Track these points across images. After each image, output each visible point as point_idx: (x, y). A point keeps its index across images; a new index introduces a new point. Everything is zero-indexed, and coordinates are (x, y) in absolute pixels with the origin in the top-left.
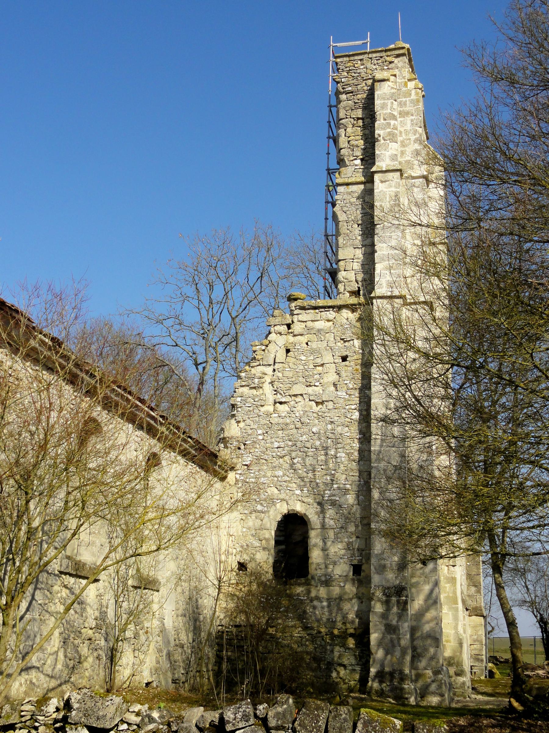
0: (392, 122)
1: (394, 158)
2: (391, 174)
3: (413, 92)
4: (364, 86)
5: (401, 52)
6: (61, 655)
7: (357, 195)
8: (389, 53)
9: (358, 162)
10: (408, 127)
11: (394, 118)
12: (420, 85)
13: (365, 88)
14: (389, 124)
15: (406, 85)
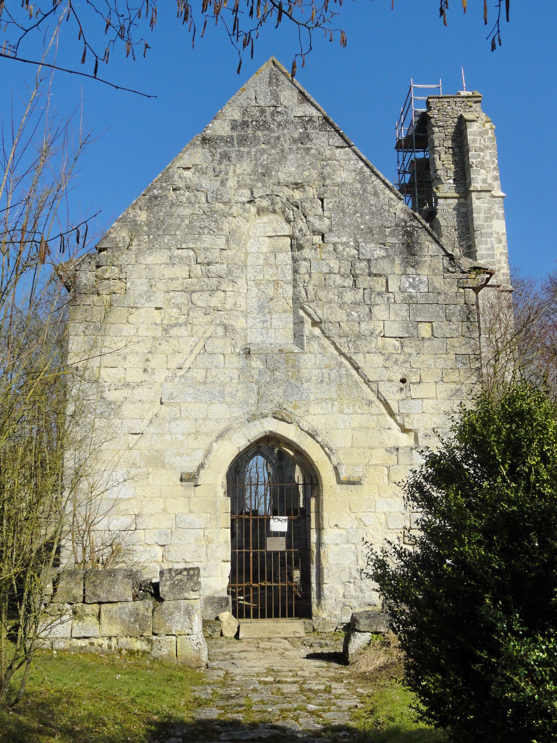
0: (482, 154)
1: (484, 181)
2: (484, 193)
3: (490, 131)
4: (452, 123)
5: (478, 99)
7: (452, 207)
8: (469, 99)
9: (451, 181)
10: (488, 158)
11: (482, 150)
12: (494, 127)
13: (453, 124)
14: (479, 155)
15: (484, 126)
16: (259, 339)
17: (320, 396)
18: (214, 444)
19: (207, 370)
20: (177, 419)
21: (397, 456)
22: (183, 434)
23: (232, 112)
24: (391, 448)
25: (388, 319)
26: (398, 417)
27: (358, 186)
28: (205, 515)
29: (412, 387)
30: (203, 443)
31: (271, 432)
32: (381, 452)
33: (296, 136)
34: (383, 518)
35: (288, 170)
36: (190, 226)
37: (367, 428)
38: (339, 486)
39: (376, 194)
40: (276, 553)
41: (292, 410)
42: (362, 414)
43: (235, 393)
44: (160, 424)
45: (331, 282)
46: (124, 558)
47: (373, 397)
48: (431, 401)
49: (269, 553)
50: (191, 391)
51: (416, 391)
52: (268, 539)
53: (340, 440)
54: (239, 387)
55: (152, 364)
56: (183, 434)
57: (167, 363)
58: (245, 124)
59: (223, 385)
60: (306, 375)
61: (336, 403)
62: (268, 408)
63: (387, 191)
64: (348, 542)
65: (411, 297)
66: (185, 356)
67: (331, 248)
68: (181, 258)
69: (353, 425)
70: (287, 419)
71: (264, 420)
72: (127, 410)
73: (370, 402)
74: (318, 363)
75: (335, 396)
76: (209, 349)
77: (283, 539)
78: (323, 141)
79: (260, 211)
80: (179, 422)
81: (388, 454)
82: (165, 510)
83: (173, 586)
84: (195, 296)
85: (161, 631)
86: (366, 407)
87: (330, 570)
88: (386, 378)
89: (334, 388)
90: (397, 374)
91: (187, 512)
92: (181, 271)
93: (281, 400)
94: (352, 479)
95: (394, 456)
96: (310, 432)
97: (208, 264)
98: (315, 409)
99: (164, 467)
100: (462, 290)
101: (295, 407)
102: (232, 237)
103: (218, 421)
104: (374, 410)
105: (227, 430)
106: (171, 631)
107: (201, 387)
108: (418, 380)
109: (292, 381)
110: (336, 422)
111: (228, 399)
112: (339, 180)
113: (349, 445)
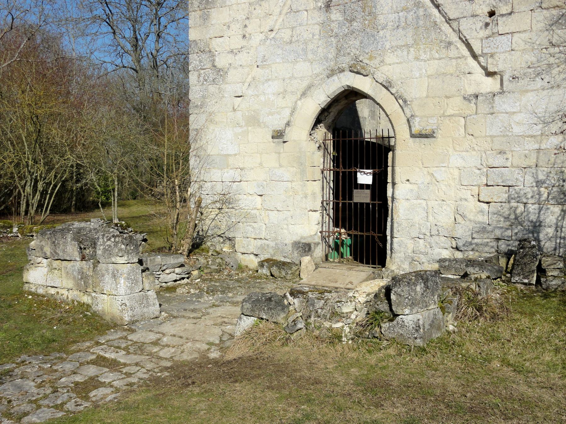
17: (394, 44)
18: (299, 102)
19: (293, 28)
20: (269, 80)
21: (476, 104)
22: (274, 94)
24: (470, 95)
26: (481, 59)
28: (292, 169)
29: (501, 20)
30: (289, 101)
31: (348, 86)
32: (458, 101)
34: (456, 172)
37: (444, 74)
38: (412, 140)
40: (362, 204)
41: (367, 62)
42: (440, 59)
43: (316, 49)
44: (256, 87)
46: (233, 205)
47: (454, 38)
48: (523, 35)
49: (356, 204)
50: (280, 52)
51: (504, 25)
52: (355, 191)
53: (415, 91)
54: (320, 42)
55: (249, 30)
56: (274, 94)
57: (260, 27)
59: (306, 43)
60: (382, 21)
61: (412, 49)
62: (346, 61)
64: (418, 198)
66: (275, 18)
69: (429, 73)
70: (362, 71)
71: (342, 75)
72: (232, 75)
73: (450, 43)
74: (394, 7)
75: (410, 41)
76: (294, 7)
77: (368, 192)
80: (270, 82)
81: (466, 103)
82: (261, 164)
83: (105, 250)
85: (97, 290)
86: (444, 51)
87: (400, 225)
88: (470, 13)
89: (410, 32)
90: (483, 7)
91: (278, 165)
93: (358, 52)
94: (424, 132)
95: (473, 105)
96: (384, 83)
98: (390, 58)
99: (259, 126)
101: (371, 58)
103: (302, 78)
104: (453, 53)
105: (309, 87)
106: (103, 290)
107: (288, 47)
108: (509, 11)
109: (368, 30)
110: (412, 71)
111: (310, 56)
113: (425, 94)
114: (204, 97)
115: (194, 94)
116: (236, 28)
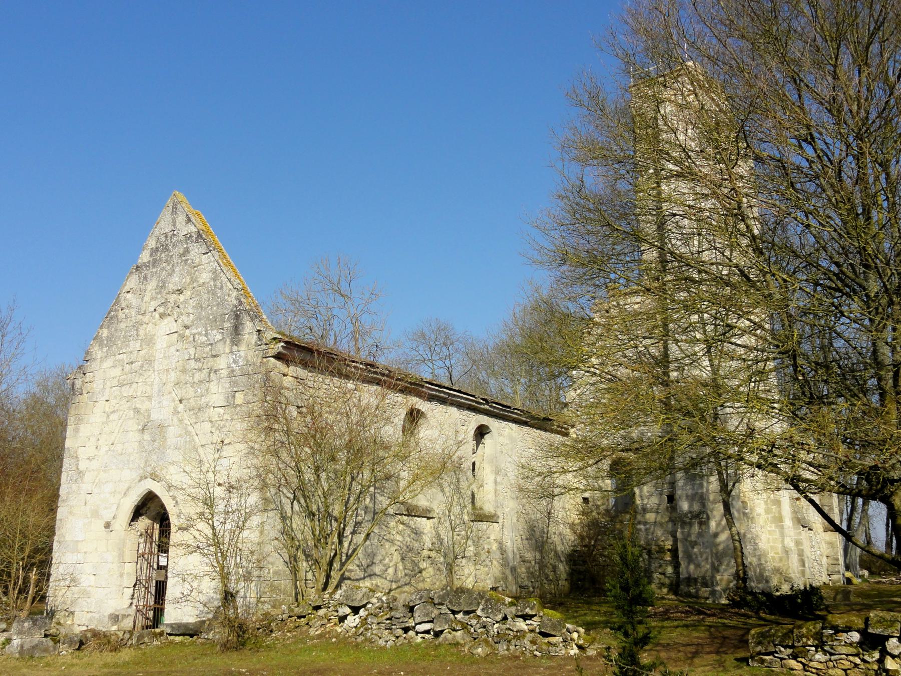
6: (400, 567)
16: (156, 417)
23: (152, 243)
25: (217, 393)
27: (212, 283)
33: (181, 251)
35: (175, 281)
36: (125, 337)
39: (222, 288)
45: (187, 367)
58: (157, 249)
63: (228, 284)
65: (233, 371)
67: (191, 339)
68: (119, 361)
72: (88, 477)
78: (196, 250)
79: (162, 316)
84: (123, 388)
92: (117, 372)
97: (132, 363)
100: (265, 360)
102: (149, 341)
112: (201, 281)
114: (68, 493)
115: (62, 492)
116: (93, 439)
